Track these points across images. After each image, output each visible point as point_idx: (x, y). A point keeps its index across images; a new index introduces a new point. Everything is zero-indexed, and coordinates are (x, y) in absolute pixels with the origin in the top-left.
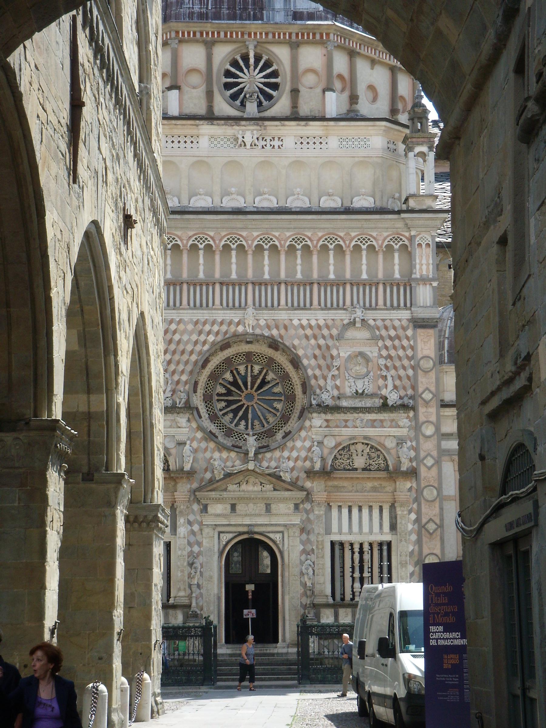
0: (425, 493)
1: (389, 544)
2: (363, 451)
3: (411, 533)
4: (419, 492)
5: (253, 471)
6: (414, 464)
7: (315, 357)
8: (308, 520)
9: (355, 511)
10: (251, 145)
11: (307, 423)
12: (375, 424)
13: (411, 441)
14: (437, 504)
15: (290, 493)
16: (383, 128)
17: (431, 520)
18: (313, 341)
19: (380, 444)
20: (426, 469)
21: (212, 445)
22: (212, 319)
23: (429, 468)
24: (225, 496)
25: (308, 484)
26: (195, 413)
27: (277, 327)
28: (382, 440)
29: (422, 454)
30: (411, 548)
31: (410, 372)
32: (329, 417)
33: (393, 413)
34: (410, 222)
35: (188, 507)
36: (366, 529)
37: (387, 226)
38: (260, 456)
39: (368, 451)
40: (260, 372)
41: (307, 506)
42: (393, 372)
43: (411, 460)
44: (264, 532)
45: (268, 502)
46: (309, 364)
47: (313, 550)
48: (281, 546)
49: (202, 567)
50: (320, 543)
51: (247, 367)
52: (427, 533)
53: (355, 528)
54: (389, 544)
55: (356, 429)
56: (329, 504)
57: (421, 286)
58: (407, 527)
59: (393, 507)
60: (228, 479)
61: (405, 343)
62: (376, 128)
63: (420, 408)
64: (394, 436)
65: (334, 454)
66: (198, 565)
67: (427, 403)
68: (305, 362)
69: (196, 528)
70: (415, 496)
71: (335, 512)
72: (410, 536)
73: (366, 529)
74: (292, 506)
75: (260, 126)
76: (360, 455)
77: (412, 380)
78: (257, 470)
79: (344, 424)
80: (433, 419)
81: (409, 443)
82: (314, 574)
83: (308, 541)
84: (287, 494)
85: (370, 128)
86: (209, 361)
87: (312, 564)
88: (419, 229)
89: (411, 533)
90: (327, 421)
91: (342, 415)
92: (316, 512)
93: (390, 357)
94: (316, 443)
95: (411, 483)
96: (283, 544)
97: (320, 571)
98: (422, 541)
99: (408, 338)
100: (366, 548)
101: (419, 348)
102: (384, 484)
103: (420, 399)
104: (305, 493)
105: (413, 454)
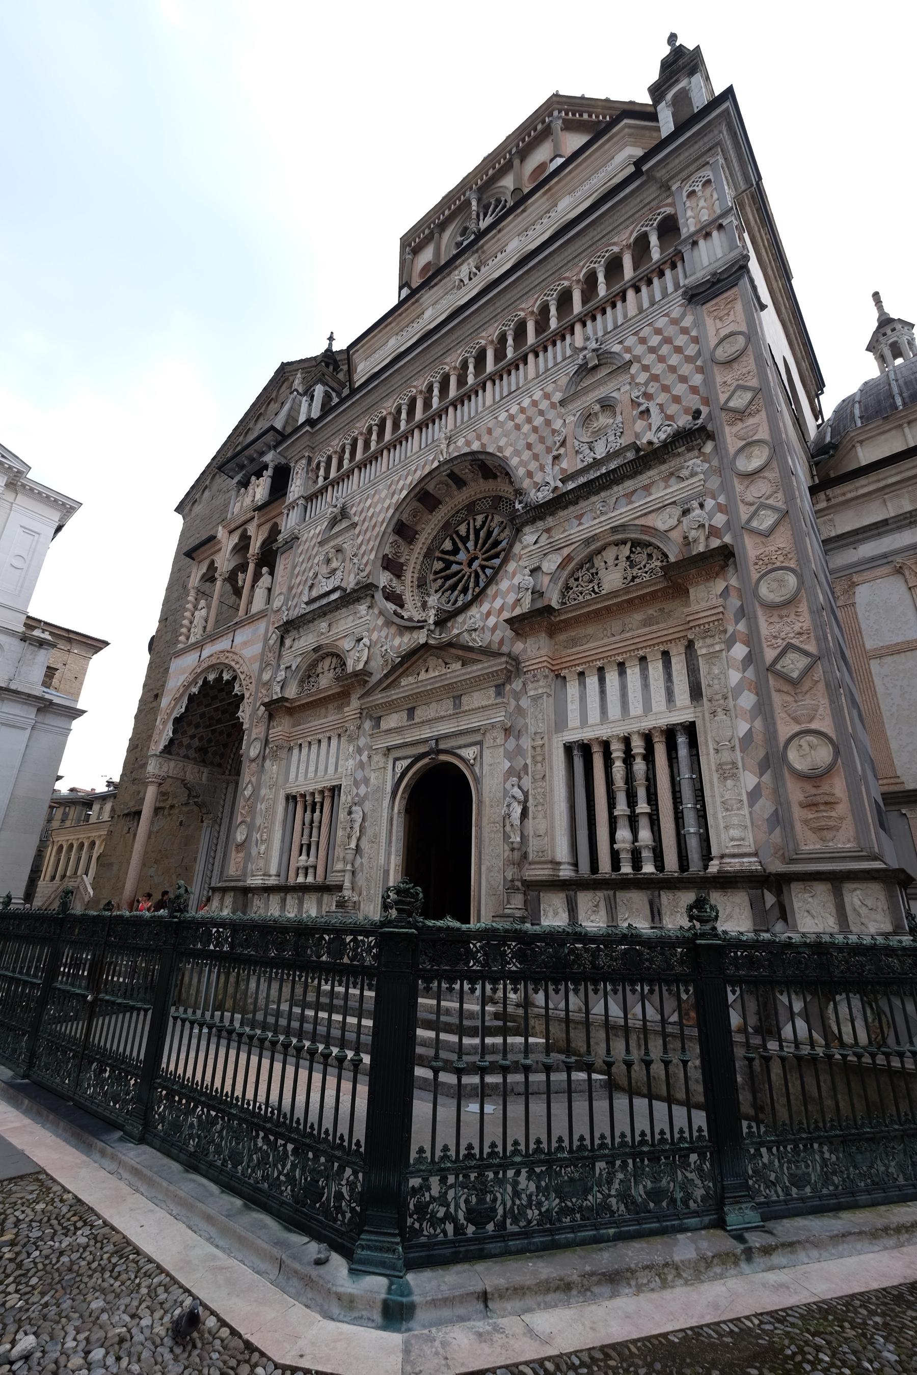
0: (763, 590)
1: (690, 729)
2: (617, 559)
3: (737, 691)
4: (749, 593)
5: (426, 644)
6: (727, 539)
7: (529, 446)
8: (518, 707)
9: (612, 677)
10: (470, 279)
11: (517, 548)
12: (633, 499)
13: (714, 498)
14: (803, 608)
15: (480, 666)
16: (627, 130)
17: (789, 647)
18: (526, 428)
19: (645, 529)
20: (758, 540)
21: (393, 630)
22: (405, 473)
23: (767, 534)
24: (395, 697)
25: (518, 647)
26: (379, 596)
27: (479, 438)
28: (648, 521)
29: (744, 512)
30: (743, 728)
31: (697, 380)
32: (550, 521)
33: (664, 462)
34: (664, 171)
35: (359, 728)
36: (636, 708)
37: (630, 213)
38: (449, 624)
39: (628, 553)
40: (484, 523)
41: (517, 685)
42: (662, 398)
43: (714, 532)
44: (453, 748)
45: (456, 694)
46: (521, 461)
47: (526, 765)
48: (477, 769)
49: (364, 820)
50: (538, 749)
51: (468, 524)
52: (781, 681)
53: (614, 710)
54: (690, 729)
55: (597, 521)
56: (558, 676)
57: (702, 243)
58: (726, 677)
59: (690, 646)
60: (401, 670)
61: (681, 340)
62: (615, 139)
63: (727, 429)
64: (674, 503)
65: (562, 580)
66: (358, 816)
67: (740, 415)
68: (514, 461)
69: (364, 758)
70: (739, 603)
71: (573, 688)
72: (735, 698)
73: (636, 708)
74: (492, 692)
75: (477, 251)
76: (613, 568)
77: (701, 390)
78: (431, 642)
79: (576, 522)
80: (763, 433)
81: (710, 503)
82: (524, 814)
83: (519, 750)
84: (475, 670)
85: (607, 147)
86: (416, 533)
87: (520, 795)
88: (684, 174)
89: (737, 691)
90: (548, 530)
91: (571, 509)
92: (532, 693)
93: (655, 378)
94: (527, 571)
95: (725, 580)
96: (481, 764)
97: (540, 808)
98: (771, 705)
99: (685, 331)
100: (638, 747)
101: (711, 332)
102: (668, 606)
103: (723, 414)
104: (504, 659)
105: (719, 520)
